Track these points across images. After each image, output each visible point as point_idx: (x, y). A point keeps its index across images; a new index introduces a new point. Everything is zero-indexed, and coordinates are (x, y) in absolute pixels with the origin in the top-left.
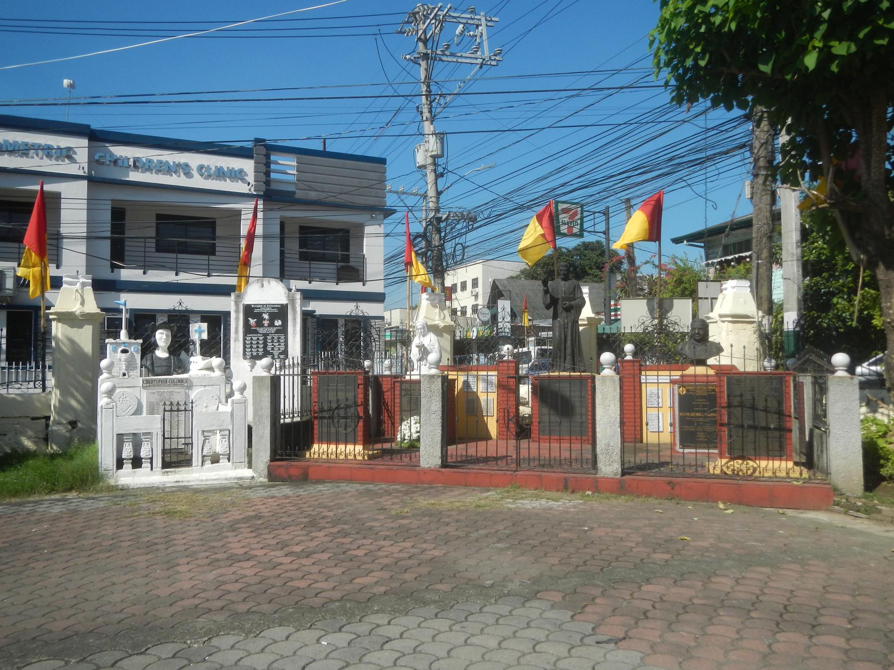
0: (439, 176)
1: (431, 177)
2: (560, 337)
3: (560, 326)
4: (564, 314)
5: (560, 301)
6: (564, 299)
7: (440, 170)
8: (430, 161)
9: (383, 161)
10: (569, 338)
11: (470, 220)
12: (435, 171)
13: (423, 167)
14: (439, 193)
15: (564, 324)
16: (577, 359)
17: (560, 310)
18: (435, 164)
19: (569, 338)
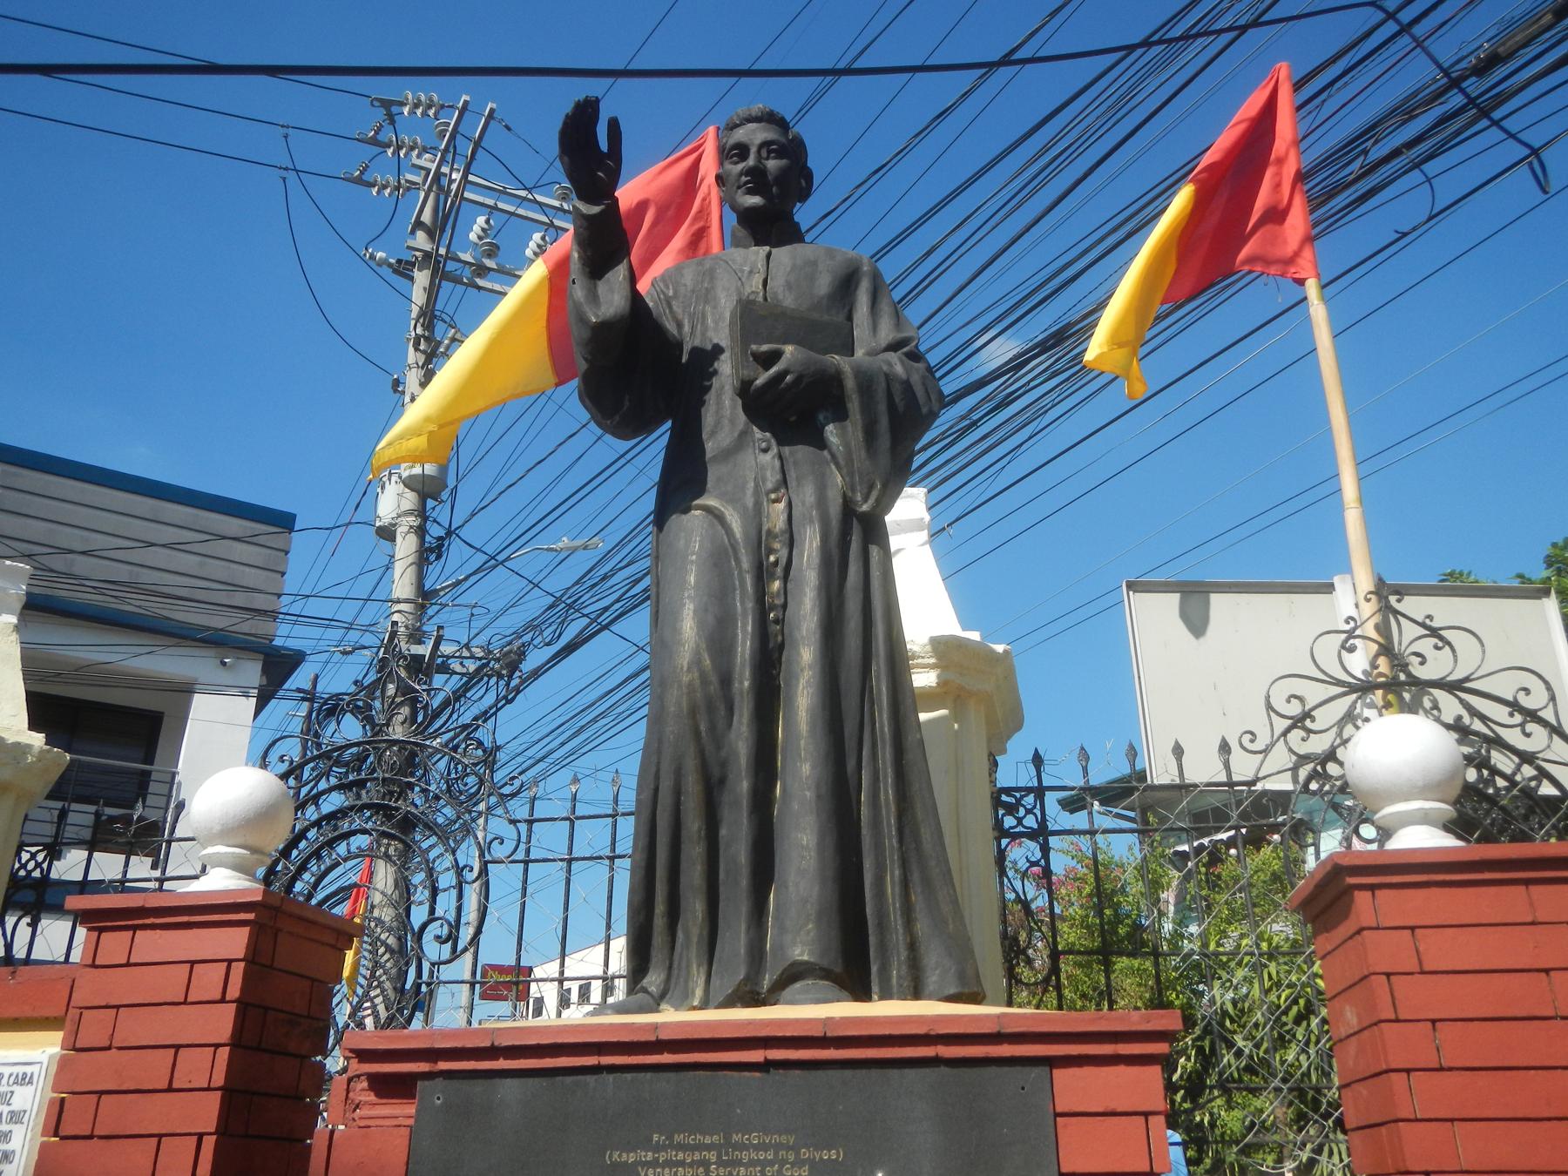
0: (428, 553)
1: (406, 546)
2: (718, 639)
3: (720, 559)
4: (761, 459)
5: (725, 367)
6: (755, 318)
7: (435, 531)
8: (410, 500)
9: (285, 521)
10: (805, 655)
11: (507, 669)
12: (421, 531)
13: (387, 533)
14: (425, 597)
15: (760, 542)
16: (883, 882)
17: (722, 413)
18: (422, 513)
19: (805, 655)
